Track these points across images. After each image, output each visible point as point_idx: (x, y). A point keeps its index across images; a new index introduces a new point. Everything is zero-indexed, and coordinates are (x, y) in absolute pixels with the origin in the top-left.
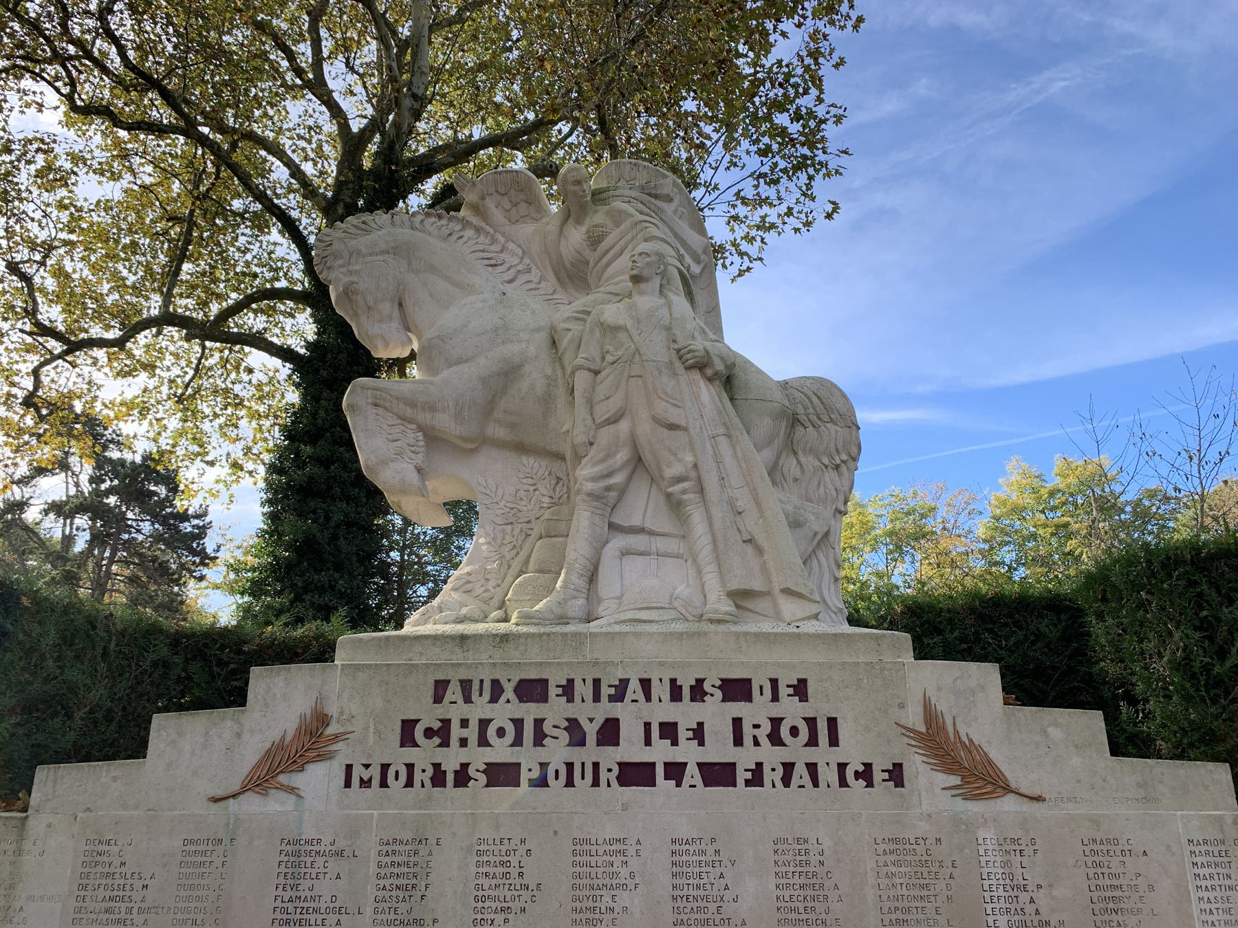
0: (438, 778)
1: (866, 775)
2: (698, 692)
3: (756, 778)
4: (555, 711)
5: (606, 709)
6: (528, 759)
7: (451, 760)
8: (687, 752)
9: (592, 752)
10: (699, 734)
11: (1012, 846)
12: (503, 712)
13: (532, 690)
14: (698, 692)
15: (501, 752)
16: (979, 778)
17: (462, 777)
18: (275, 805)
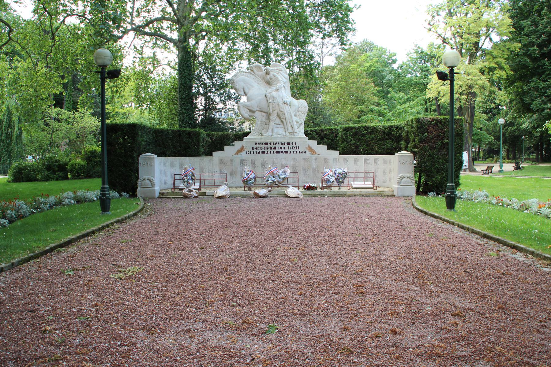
0: (256, 153)
1: (302, 152)
2: (284, 144)
3: (290, 153)
4: (269, 146)
5: (275, 146)
6: (266, 151)
7: (258, 151)
8: (283, 150)
9: (273, 150)
10: (284, 148)
11: (316, 159)
12: (263, 146)
13: (266, 144)
14: (284, 144)
15: (263, 150)
16: (313, 152)
17: (259, 153)
18: (239, 156)
